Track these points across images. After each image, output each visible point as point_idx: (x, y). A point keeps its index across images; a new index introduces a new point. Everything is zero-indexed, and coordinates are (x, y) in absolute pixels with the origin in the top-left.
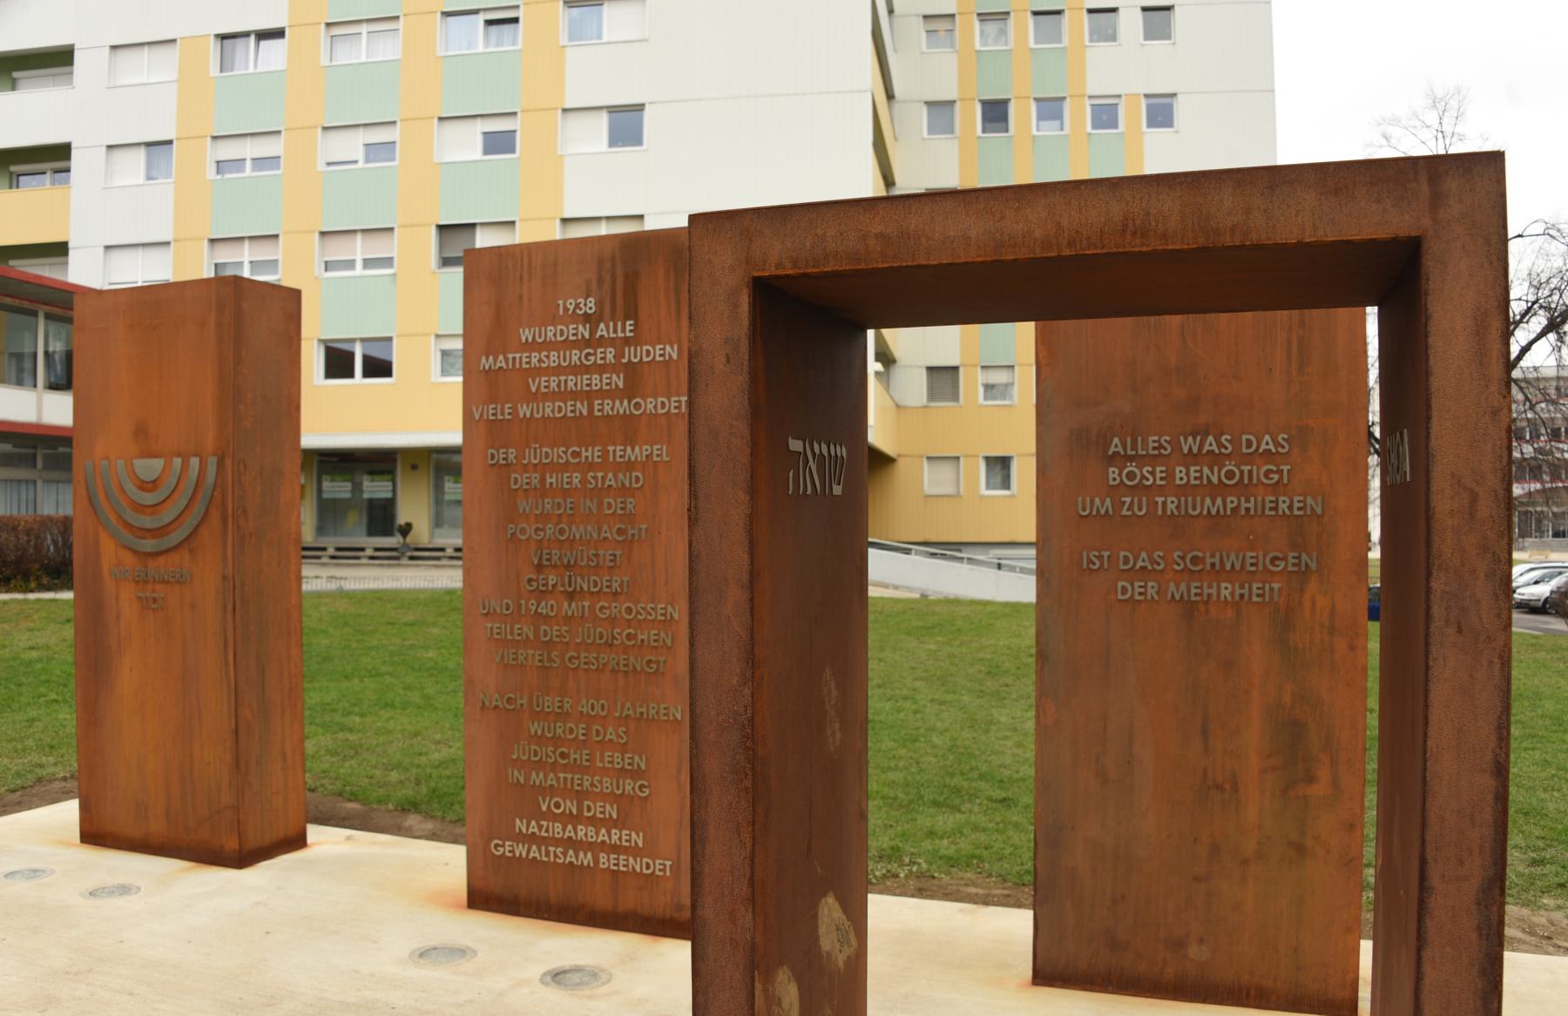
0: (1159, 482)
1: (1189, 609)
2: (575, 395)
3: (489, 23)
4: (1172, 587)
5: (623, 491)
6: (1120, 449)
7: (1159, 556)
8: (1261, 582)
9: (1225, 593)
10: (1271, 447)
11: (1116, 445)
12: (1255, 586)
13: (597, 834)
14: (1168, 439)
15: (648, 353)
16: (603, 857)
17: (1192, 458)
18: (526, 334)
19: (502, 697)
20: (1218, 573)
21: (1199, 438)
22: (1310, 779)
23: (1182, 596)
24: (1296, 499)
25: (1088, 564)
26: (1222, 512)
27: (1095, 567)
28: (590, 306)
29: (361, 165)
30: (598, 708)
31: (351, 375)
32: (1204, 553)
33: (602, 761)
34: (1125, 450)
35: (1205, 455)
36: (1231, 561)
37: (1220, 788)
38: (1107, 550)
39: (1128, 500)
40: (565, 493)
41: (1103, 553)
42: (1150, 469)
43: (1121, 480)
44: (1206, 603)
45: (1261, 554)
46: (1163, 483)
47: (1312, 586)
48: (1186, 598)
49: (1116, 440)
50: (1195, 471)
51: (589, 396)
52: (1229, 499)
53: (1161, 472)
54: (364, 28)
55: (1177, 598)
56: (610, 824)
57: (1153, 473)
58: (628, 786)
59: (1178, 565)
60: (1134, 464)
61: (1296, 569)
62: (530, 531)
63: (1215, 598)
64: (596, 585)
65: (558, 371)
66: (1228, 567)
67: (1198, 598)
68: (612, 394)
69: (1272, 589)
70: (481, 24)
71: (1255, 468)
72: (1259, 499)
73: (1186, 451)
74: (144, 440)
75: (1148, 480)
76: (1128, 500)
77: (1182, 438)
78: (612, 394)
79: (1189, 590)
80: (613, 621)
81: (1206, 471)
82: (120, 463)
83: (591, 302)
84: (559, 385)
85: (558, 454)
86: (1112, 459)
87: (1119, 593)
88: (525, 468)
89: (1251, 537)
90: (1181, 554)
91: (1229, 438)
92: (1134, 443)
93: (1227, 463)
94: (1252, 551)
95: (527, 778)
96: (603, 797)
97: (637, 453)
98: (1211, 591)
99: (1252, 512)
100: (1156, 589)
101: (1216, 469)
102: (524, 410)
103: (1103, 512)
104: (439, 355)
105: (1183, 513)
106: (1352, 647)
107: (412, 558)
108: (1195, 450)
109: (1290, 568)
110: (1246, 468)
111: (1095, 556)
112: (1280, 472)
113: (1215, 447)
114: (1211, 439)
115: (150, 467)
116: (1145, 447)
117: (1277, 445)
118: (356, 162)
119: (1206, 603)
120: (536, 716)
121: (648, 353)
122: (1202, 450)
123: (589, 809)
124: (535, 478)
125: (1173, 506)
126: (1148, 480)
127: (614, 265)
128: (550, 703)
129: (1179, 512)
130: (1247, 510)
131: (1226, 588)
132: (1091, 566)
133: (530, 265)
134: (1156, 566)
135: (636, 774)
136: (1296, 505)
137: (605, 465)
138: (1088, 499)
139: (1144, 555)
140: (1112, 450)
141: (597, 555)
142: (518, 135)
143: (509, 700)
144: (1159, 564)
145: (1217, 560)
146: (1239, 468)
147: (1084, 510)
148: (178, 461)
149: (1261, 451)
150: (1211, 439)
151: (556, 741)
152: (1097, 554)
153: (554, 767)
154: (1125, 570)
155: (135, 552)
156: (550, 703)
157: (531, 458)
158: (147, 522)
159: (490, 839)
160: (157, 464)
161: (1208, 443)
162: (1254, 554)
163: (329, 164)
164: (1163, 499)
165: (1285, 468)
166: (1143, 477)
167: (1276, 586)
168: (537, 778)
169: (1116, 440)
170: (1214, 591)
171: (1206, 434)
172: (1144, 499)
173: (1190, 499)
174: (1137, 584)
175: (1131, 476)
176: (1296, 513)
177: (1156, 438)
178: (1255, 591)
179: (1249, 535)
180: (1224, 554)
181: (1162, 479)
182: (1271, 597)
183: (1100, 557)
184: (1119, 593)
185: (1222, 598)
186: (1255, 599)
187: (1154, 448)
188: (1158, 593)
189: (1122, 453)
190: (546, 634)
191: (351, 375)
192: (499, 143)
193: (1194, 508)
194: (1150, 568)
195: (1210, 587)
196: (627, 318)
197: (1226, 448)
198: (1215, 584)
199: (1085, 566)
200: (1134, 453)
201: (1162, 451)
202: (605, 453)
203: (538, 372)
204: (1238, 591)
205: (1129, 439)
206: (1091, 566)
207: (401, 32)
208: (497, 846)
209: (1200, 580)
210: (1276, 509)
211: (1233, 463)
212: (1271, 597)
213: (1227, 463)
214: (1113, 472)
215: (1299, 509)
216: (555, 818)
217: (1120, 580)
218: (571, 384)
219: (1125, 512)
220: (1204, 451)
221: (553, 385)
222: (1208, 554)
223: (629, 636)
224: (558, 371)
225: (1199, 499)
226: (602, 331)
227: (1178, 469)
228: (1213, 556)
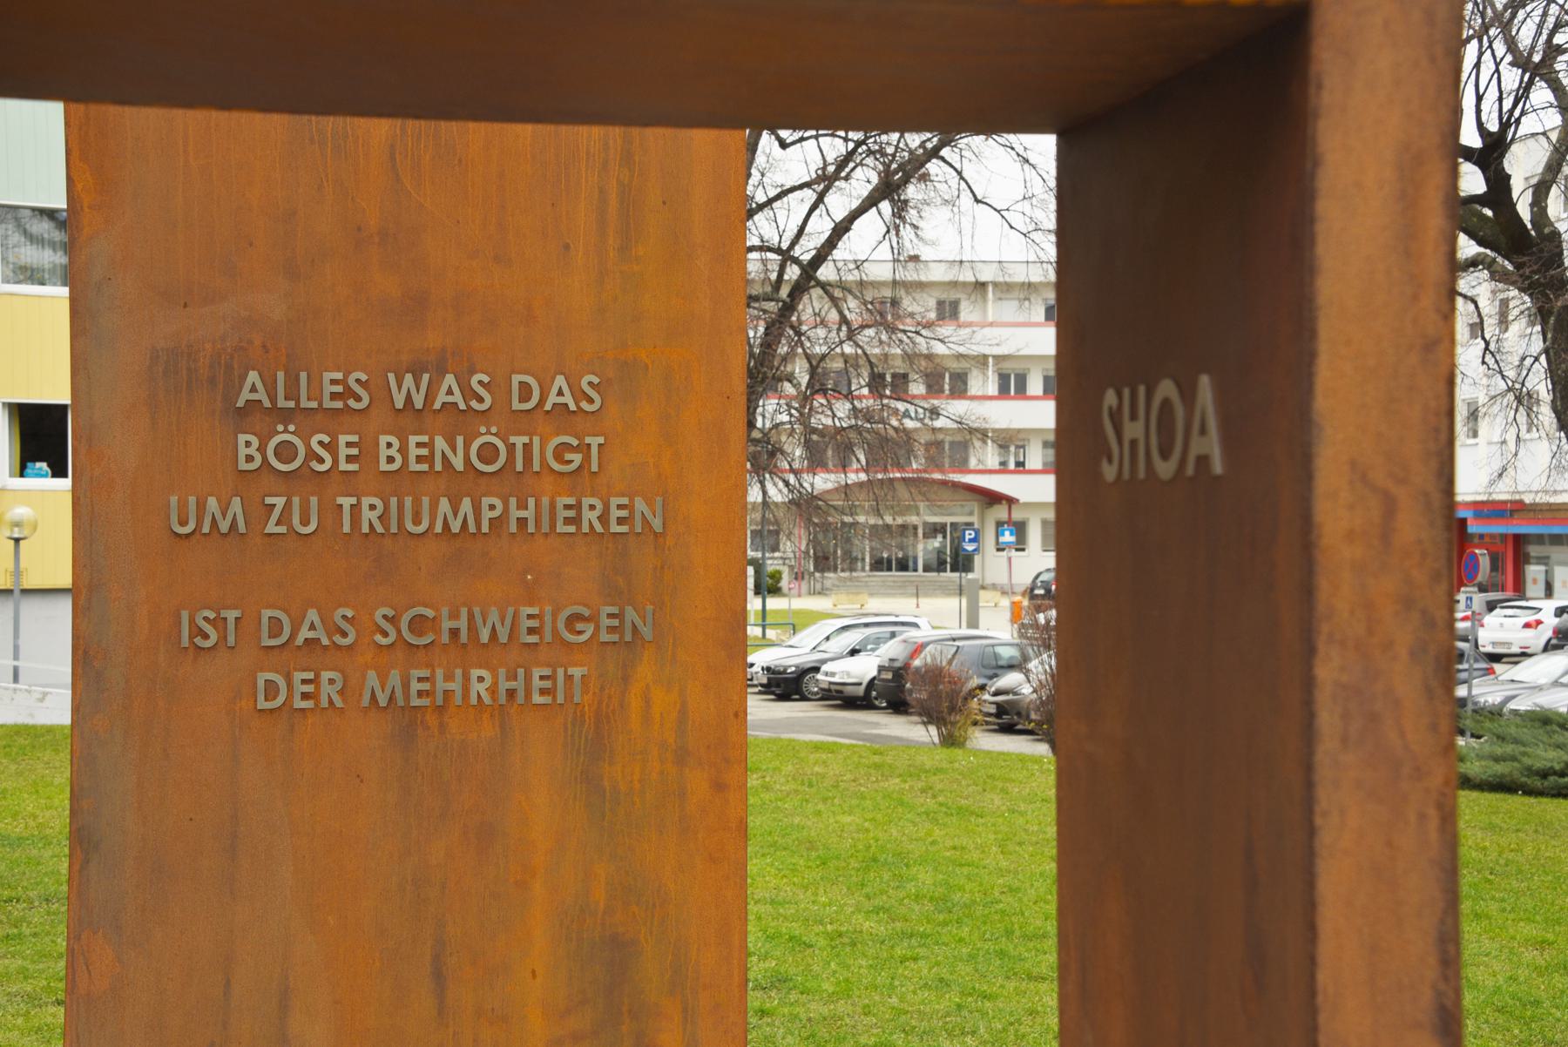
0: (343, 466)
4: (372, 679)
6: (261, 395)
7: (344, 617)
8: (548, 666)
10: (568, 399)
11: (252, 386)
12: (537, 673)
14: (364, 377)
17: (411, 417)
20: (464, 648)
21: (426, 377)
23: (392, 698)
24: (614, 501)
25: (191, 638)
26: (472, 528)
27: (208, 644)
32: (437, 610)
34: (273, 399)
35: (439, 411)
36: (489, 625)
38: (235, 608)
39: (279, 502)
41: (224, 614)
42: (326, 439)
43: (265, 459)
44: (440, 710)
45: (548, 609)
46: (353, 467)
47: (645, 670)
48: (401, 702)
49: (253, 376)
50: (419, 445)
52: (486, 501)
53: (349, 445)
55: (383, 702)
57: (331, 447)
59: (385, 634)
60: (292, 428)
61: (615, 637)
63: (458, 699)
66: (485, 636)
67: (425, 702)
69: (569, 678)
71: (536, 440)
72: (545, 501)
73: (399, 404)
75: (321, 461)
76: (279, 502)
77: (391, 376)
79: (406, 686)
81: (440, 443)
87: (261, 697)
89: (529, 577)
90: (390, 613)
91: (486, 379)
93: (483, 430)
94: (531, 605)
98: (450, 686)
99: (531, 528)
100: (339, 685)
101: (460, 440)
103: (224, 526)
105: (394, 530)
106: (719, 787)
108: (419, 402)
109: (605, 637)
110: (519, 441)
111: (206, 619)
112: (585, 449)
113: (457, 397)
114: (450, 379)
116: (315, 392)
117: (580, 395)
119: (440, 710)
122: (433, 404)
125: (374, 515)
126: (321, 461)
129: (387, 528)
130: (522, 522)
131: (481, 679)
132: (198, 641)
134: (338, 639)
136: (616, 513)
138: (192, 500)
139: (313, 615)
140: (245, 395)
144: (344, 634)
145: (463, 624)
146: (505, 441)
147: (183, 523)
149: (548, 407)
150: (450, 379)
152: (212, 615)
154: (272, 647)
161: (444, 388)
162: (534, 611)
164: (353, 500)
165: (595, 441)
166: (312, 455)
167: (576, 672)
169: (253, 376)
170: (455, 686)
171: (441, 372)
172: (314, 500)
173: (408, 501)
174: (299, 676)
175: (287, 452)
176: (615, 528)
177: (339, 376)
178: (537, 683)
179: (526, 572)
180: (477, 610)
181: (350, 459)
182: (569, 695)
184: (261, 697)
185: (474, 700)
186: (537, 699)
187: (334, 396)
188: (341, 692)
189: (267, 404)
193: (417, 522)
194: (325, 641)
195: (449, 677)
197: (481, 400)
198: (458, 672)
199: (185, 642)
200: (292, 404)
201: (352, 403)
204: (504, 685)
205: (281, 375)
206: (198, 641)
209: (430, 665)
210: (575, 521)
211: (494, 430)
212: (569, 695)
213: (483, 430)
214: (246, 444)
215: (620, 521)
217: (262, 670)
219: (271, 528)
220: (437, 406)
222: (445, 611)
225: (426, 500)
227: (384, 439)
228: (454, 615)
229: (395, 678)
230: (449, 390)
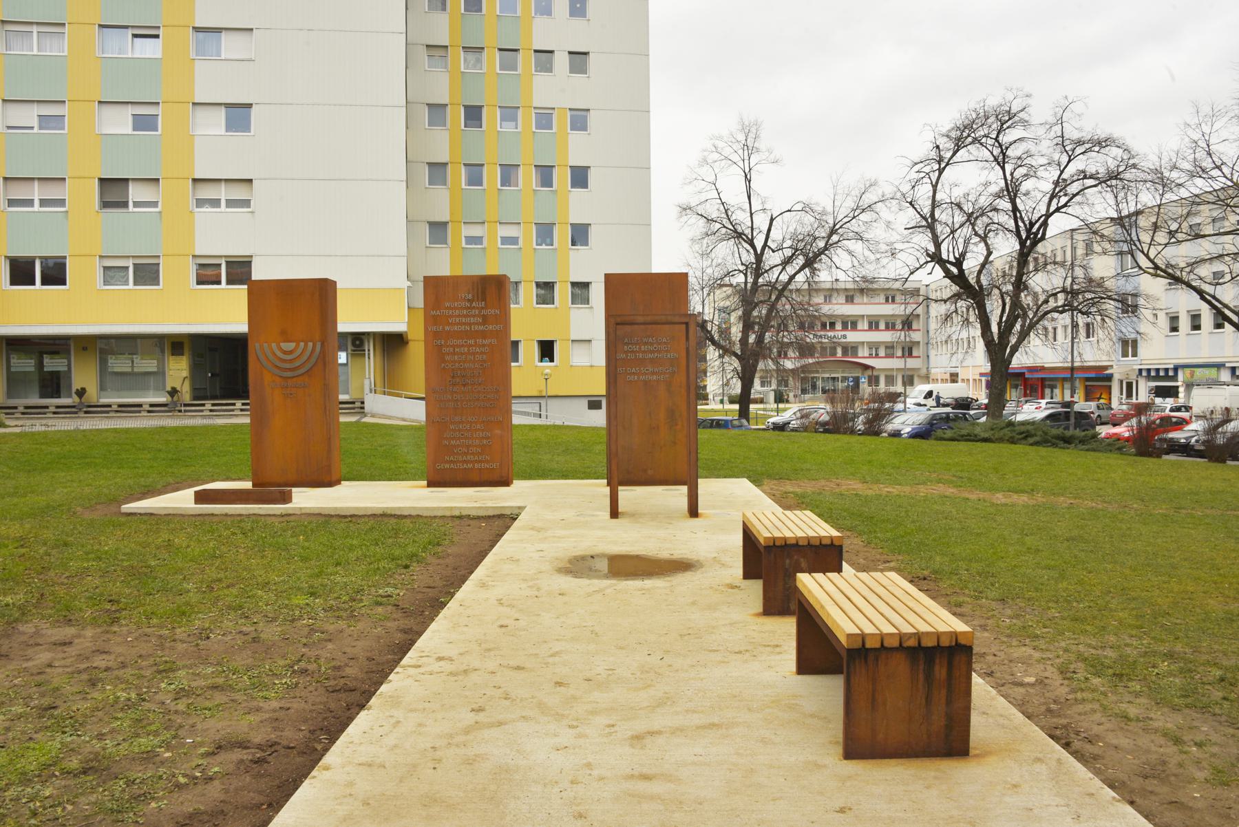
1: (646, 383)
2: (465, 324)
5: (482, 353)
11: (626, 340)
17: (646, 344)
18: (447, 304)
22: (677, 425)
28: (470, 297)
29: (36, 130)
31: (33, 283)
51: (470, 324)
54: (35, 29)
58: (485, 442)
65: (459, 316)
70: (130, 36)
80: (479, 392)
82: (274, 345)
83: (470, 295)
85: (459, 342)
97: (486, 342)
102: (447, 328)
104: (102, 269)
107: (86, 412)
118: (32, 128)
124: (451, 350)
128: (457, 419)
135: (488, 438)
137: (476, 345)
142: (160, 118)
151: (459, 430)
153: (459, 438)
156: (457, 419)
157: (449, 343)
158: (288, 366)
160: (291, 346)
163: (9, 127)
168: (453, 442)
191: (33, 283)
192: (144, 123)
202: (476, 342)
207: (66, 35)
214: (626, 347)
216: (460, 454)
224: (459, 316)
226: (474, 304)
230: (650, 340)
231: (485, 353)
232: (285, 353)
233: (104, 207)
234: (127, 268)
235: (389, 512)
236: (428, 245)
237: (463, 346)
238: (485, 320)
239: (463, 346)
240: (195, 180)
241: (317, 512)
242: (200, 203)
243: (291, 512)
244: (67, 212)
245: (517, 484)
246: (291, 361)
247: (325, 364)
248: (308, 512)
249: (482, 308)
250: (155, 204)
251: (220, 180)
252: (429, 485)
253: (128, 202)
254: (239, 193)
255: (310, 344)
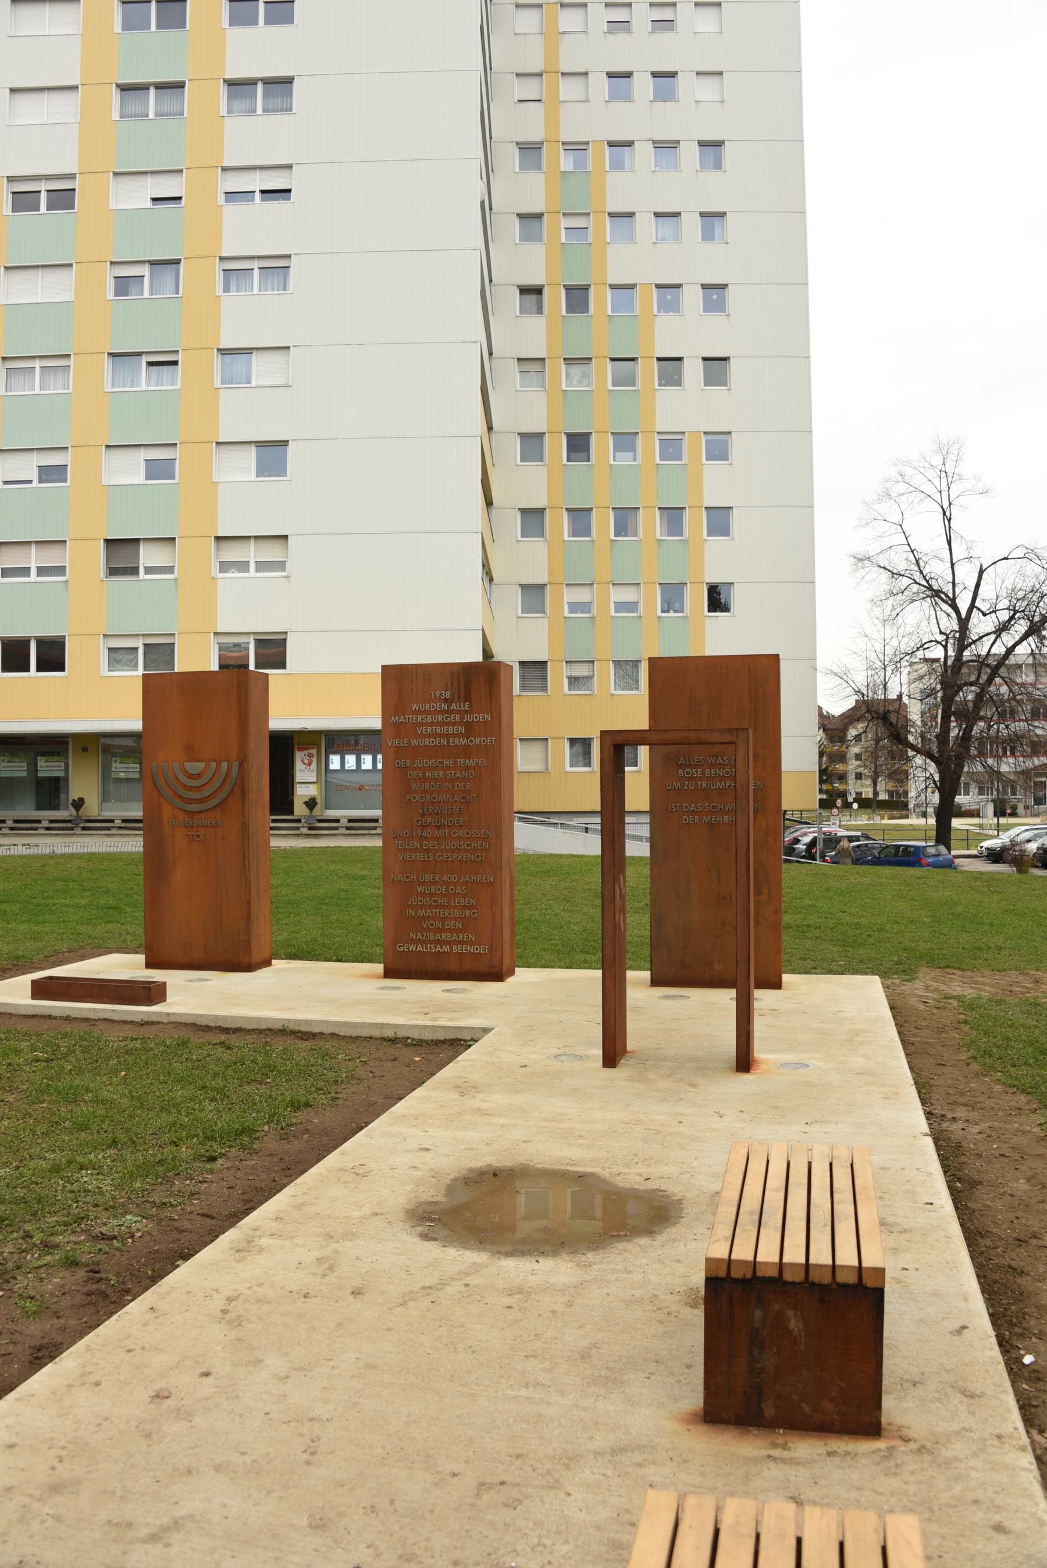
1: (711, 826)
2: (440, 736)
3: (150, 364)
5: (465, 779)
9: (726, 820)
11: (682, 760)
13: (452, 936)
15: (476, 717)
16: (455, 947)
17: (712, 766)
18: (415, 707)
19: (403, 876)
20: (723, 812)
29: (35, 484)
30: (452, 878)
31: (27, 669)
33: (454, 902)
37: (725, 898)
40: (436, 780)
51: (447, 736)
54: (37, 364)
56: (459, 931)
58: (468, 913)
62: (418, 798)
64: (451, 822)
65: (431, 724)
68: (458, 735)
70: (144, 365)
74: (191, 752)
78: (458, 735)
80: (459, 838)
82: (176, 765)
83: (448, 693)
84: (432, 731)
86: (681, 766)
88: (415, 769)
92: (689, 759)
95: (416, 913)
96: (455, 919)
97: (471, 762)
102: (414, 742)
104: (106, 651)
107: (84, 829)
115: (198, 767)
118: (30, 482)
120: (420, 883)
121: (476, 717)
123: (448, 925)
127: (459, 678)
128: (427, 877)
133: (416, 675)
135: (471, 907)
141: (452, 809)
142: (177, 462)
143: (407, 877)
148: (213, 764)
151: (431, 895)
153: (430, 907)
155: (185, 811)
156: (427, 877)
157: (418, 764)
158: (194, 795)
159: (396, 945)
160: (200, 766)
163: (6, 483)
168: (421, 913)
175: (688, 773)
183: (676, 806)
190: (426, 845)
191: (28, 670)
192: (157, 470)
196: (466, 701)
203: (422, 724)
207: (72, 368)
208: (400, 946)
214: (681, 771)
218: (438, 731)
221: (429, 731)
223: (468, 845)
224: (431, 724)
226: (453, 706)
229: (709, 817)
230: (719, 760)
231: (469, 780)
232: (191, 776)
233: (110, 574)
234: (136, 649)
235: (291, 1027)
236: (520, 614)
237: (436, 768)
238: (470, 729)
239: (436, 768)
240: (218, 539)
241: (190, 1021)
242: (225, 567)
243: (154, 1019)
244: (67, 581)
245: (523, 976)
246: (198, 788)
247: (244, 793)
248: (179, 1020)
249: (466, 712)
250: (169, 570)
251: (248, 538)
252: (389, 974)
253: (138, 567)
254: (271, 553)
255: (225, 765)
